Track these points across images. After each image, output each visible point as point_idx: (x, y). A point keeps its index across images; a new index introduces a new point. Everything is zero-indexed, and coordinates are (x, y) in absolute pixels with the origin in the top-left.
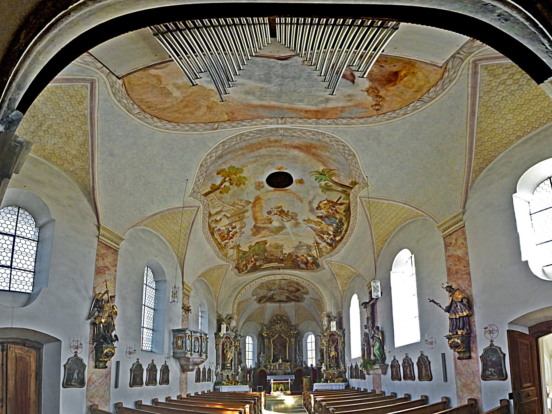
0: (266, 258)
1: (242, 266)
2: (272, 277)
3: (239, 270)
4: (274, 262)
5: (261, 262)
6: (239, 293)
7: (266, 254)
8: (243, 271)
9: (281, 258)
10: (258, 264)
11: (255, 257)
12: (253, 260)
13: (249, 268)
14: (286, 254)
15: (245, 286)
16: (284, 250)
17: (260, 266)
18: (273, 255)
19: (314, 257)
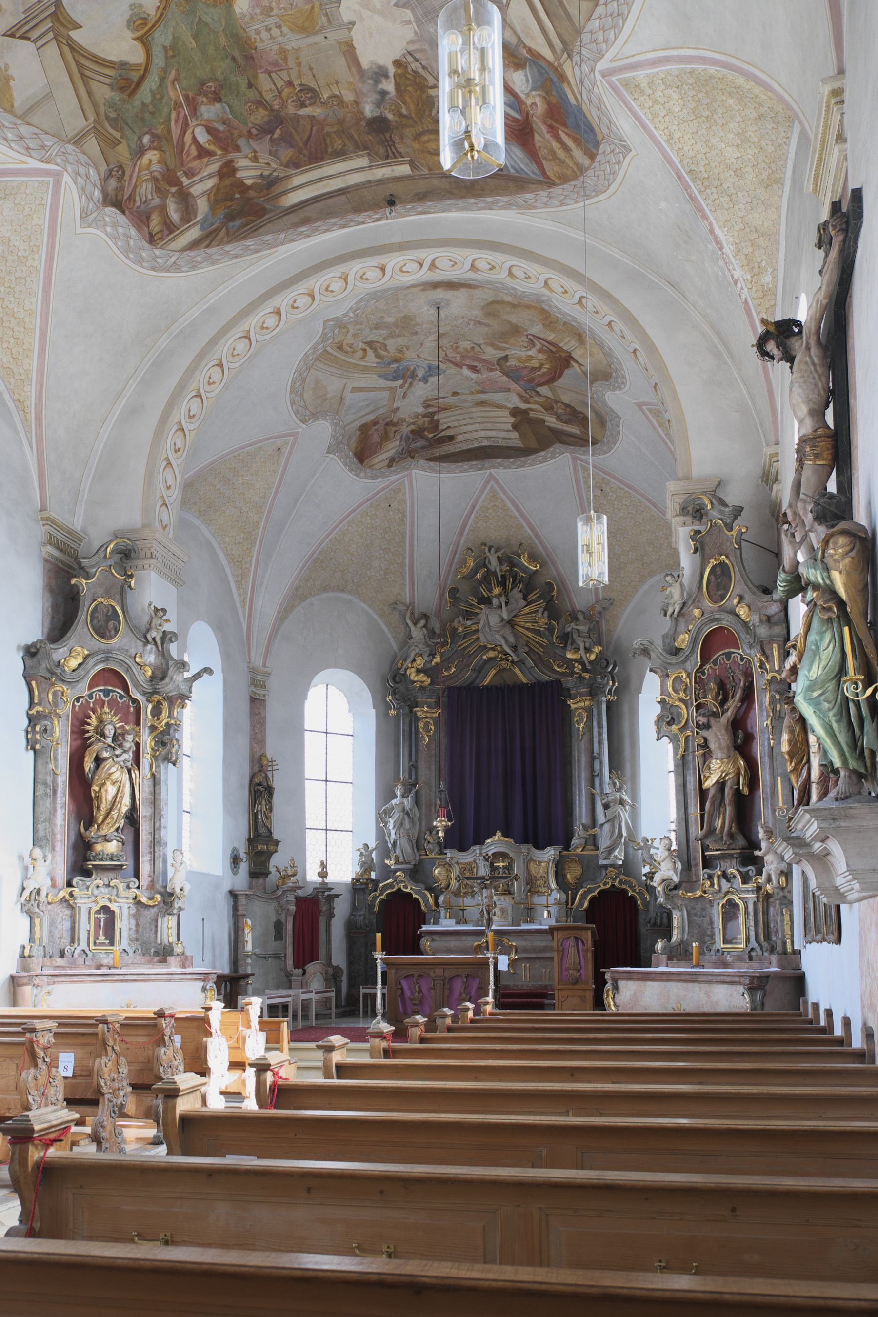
0: (277, 120)
1: (146, 189)
2: (365, 277)
3: (141, 219)
4: (341, 154)
5: (263, 147)
6: (181, 386)
7: (264, 83)
8: (169, 228)
9: (369, 110)
10: (248, 172)
11: (209, 111)
12: (202, 137)
13: (202, 206)
14: (380, 73)
15: (213, 342)
16: (357, 36)
17: (270, 184)
18: (309, 95)
19: (536, 57)
